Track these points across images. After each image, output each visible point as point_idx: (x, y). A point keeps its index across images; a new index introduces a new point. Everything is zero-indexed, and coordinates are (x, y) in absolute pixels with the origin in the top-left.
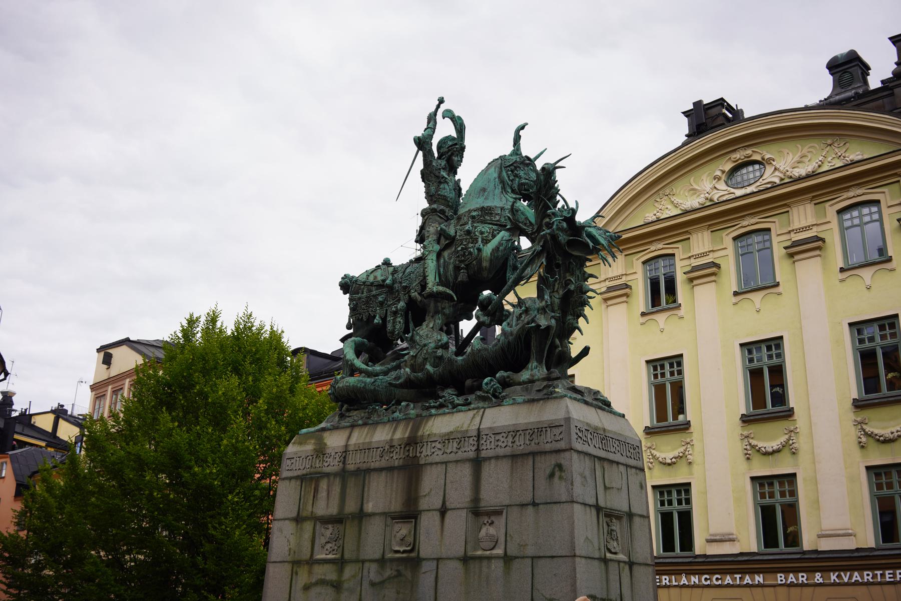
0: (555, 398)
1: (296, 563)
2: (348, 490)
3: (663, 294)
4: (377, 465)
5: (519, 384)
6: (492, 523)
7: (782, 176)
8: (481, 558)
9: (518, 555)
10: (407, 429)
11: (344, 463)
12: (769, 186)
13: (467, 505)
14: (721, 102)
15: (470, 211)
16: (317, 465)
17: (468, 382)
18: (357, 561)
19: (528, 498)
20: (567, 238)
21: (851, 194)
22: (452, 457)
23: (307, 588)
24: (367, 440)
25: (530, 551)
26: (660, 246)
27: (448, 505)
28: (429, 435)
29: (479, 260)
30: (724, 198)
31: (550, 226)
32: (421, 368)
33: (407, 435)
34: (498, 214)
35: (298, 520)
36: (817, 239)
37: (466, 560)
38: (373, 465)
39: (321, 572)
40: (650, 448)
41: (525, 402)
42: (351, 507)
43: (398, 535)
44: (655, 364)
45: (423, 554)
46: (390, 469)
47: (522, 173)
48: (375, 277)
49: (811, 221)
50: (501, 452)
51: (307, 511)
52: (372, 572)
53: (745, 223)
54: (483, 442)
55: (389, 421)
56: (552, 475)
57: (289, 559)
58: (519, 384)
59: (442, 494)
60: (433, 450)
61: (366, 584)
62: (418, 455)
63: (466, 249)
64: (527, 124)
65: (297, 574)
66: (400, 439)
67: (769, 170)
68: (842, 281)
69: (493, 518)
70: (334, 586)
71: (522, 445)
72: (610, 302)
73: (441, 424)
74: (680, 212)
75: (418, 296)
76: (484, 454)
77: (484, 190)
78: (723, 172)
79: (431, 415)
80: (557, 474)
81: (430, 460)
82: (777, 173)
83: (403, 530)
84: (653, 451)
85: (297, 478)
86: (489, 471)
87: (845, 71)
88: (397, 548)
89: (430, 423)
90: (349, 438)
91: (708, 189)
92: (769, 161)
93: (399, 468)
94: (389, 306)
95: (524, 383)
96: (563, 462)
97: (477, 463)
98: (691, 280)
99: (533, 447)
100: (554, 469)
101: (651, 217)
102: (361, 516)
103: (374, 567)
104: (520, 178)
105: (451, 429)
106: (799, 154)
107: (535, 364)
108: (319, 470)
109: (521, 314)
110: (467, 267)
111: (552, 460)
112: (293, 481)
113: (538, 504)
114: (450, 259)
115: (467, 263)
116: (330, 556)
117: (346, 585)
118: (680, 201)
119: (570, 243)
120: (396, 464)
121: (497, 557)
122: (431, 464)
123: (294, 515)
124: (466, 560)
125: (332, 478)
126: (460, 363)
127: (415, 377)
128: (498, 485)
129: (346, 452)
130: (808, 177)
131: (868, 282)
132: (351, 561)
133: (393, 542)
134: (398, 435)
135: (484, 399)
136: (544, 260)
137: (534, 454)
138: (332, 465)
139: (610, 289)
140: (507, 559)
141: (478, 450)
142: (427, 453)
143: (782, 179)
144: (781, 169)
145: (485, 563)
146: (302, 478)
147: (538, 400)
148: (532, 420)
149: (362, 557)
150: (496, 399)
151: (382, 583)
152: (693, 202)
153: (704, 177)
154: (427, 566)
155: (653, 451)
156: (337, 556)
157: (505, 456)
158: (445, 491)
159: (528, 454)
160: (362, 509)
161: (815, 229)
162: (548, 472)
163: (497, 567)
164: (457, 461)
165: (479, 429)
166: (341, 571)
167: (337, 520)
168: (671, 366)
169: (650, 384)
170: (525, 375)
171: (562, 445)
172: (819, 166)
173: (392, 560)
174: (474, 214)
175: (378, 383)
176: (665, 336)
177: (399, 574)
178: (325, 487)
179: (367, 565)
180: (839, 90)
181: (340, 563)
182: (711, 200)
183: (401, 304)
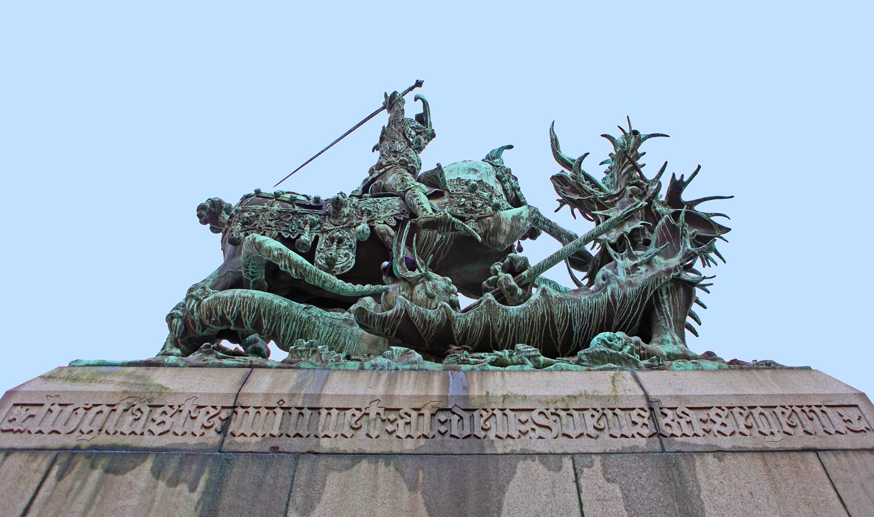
4: (343, 445)
10: (429, 383)
11: (223, 431)
16: (126, 429)
28: (505, 397)
33: (436, 390)
60: (523, 428)
64: (510, 147)
66: (411, 397)
75: (390, 229)
109: (636, 265)
120: (409, 446)
127: (419, 312)
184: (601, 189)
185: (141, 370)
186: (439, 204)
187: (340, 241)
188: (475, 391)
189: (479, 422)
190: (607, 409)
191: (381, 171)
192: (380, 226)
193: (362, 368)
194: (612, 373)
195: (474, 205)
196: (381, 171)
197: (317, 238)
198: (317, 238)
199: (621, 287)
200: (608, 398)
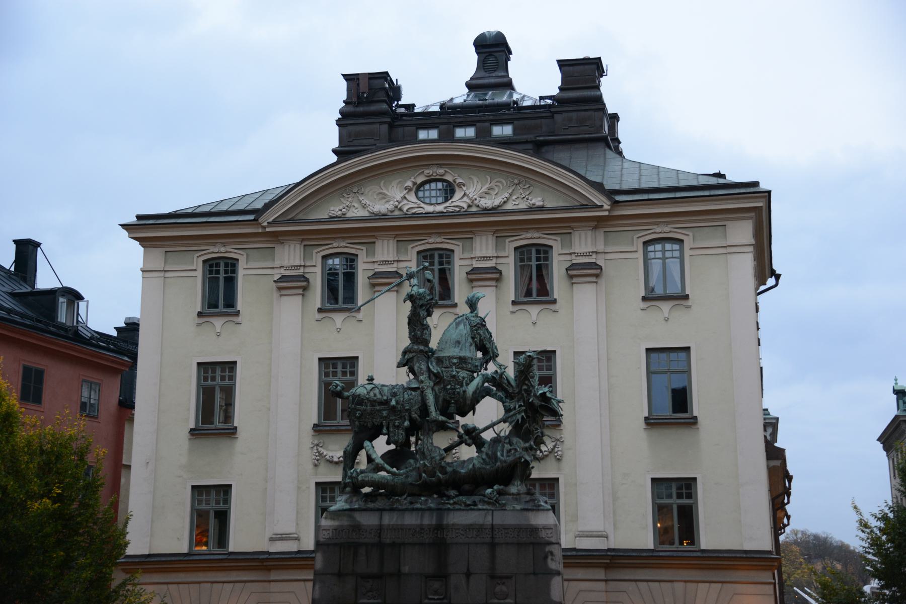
3: (340, 292)
5: (510, 494)
7: (469, 202)
11: (380, 537)
12: (457, 209)
14: (385, 76)
15: (450, 358)
21: (529, 235)
24: (399, 523)
26: (343, 244)
29: (465, 398)
30: (413, 211)
31: (528, 392)
33: (434, 522)
35: (340, 575)
36: (495, 270)
40: (317, 445)
44: (327, 363)
47: (481, 332)
48: (375, 395)
49: (491, 252)
53: (431, 240)
58: (510, 494)
67: (458, 195)
68: (513, 313)
72: (284, 292)
73: (459, 518)
74: (367, 214)
76: (496, 541)
77: (458, 342)
78: (414, 184)
82: (465, 199)
84: (320, 449)
87: (490, 54)
89: (451, 514)
91: (398, 197)
92: (460, 185)
95: (513, 494)
97: (493, 546)
98: (373, 285)
101: (335, 209)
106: (487, 186)
109: (510, 450)
110: (456, 402)
118: (368, 203)
119: (541, 406)
120: (427, 541)
130: (494, 211)
131: (534, 318)
134: (426, 521)
135: (489, 503)
137: (533, 544)
139: (283, 278)
141: (492, 538)
143: (469, 206)
144: (471, 196)
147: (532, 510)
150: (496, 504)
152: (381, 207)
153: (394, 183)
155: (320, 449)
160: (399, 570)
161: (494, 260)
164: (477, 544)
168: (344, 367)
169: (320, 380)
170: (513, 489)
171: (553, 540)
172: (505, 202)
174: (455, 361)
175: (396, 480)
176: (339, 337)
180: (482, 74)
182: (400, 209)
183: (407, 423)
187: (398, 427)
188: (445, 523)
190: (480, 528)
191: (411, 355)
192: (414, 415)
193: (413, 509)
195: (454, 393)
196: (411, 355)
200: (481, 525)
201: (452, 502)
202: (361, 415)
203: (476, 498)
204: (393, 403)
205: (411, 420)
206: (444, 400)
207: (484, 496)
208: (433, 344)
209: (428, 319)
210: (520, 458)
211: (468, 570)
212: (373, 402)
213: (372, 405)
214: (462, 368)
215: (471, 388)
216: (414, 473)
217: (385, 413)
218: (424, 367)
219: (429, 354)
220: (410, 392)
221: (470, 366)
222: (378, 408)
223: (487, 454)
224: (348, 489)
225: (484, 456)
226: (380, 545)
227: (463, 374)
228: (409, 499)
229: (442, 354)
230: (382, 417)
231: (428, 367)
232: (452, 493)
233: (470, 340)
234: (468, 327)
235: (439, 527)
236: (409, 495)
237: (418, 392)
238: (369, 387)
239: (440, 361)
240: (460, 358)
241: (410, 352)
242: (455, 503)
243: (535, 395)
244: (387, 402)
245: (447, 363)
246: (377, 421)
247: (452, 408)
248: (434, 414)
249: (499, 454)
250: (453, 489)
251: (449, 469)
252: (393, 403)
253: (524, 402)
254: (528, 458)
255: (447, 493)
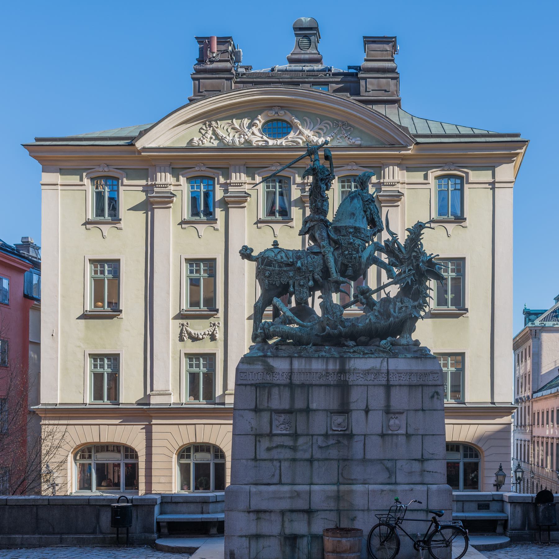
0: (430, 358)
1: (258, 436)
2: (296, 396)
4: (317, 382)
5: (400, 345)
6: (397, 418)
8: (392, 435)
9: (414, 433)
10: (336, 363)
11: (290, 379)
13: (382, 408)
15: (346, 228)
16: (268, 379)
17: (363, 339)
18: (307, 435)
19: (419, 407)
20: (427, 268)
22: (371, 383)
23: (269, 449)
24: (308, 367)
25: (421, 432)
27: (370, 407)
28: (354, 369)
29: (360, 264)
31: (417, 258)
32: (335, 328)
33: (338, 368)
34: (363, 233)
35: (256, 410)
37: (383, 435)
38: (314, 383)
39: (278, 441)
41: (412, 358)
42: (299, 404)
43: (336, 422)
45: (354, 432)
46: (328, 386)
47: (372, 207)
48: (282, 258)
50: (402, 383)
51: (265, 405)
52: (320, 441)
54: (391, 376)
55: (319, 357)
56: (432, 397)
57: (251, 433)
58: (400, 345)
59: (366, 402)
61: (315, 447)
62: (347, 379)
63: (352, 254)
65: (260, 441)
69: (397, 415)
70: (291, 448)
71: (414, 380)
73: (360, 364)
76: (391, 383)
79: (350, 358)
80: (436, 396)
81: (356, 383)
83: (339, 419)
85: (251, 385)
86: (394, 392)
88: (334, 429)
89: (352, 362)
90: (291, 364)
93: (334, 386)
94: (296, 280)
95: (403, 345)
96: (439, 391)
97: (388, 387)
99: (421, 382)
100: (434, 394)
102: (307, 411)
103: (320, 439)
104: (371, 210)
105: (369, 367)
107: (408, 335)
108: (270, 382)
109: (402, 308)
111: (433, 390)
112: (248, 388)
113: (425, 410)
114: (339, 257)
115: (352, 263)
116: (284, 432)
117: (300, 448)
119: (427, 271)
120: (332, 383)
121: (403, 435)
122: (357, 385)
123: (253, 407)
124: (383, 435)
125: (282, 388)
126: (360, 328)
128: (400, 398)
129: (291, 372)
132: (302, 435)
133: (333, 426)
134: (331, 366)
135: (384, 352)
136: (412, 277)
137: (422, 386)
138: (284, 380)
140: (408, 436)
141: (388, 380)
142: (352, 379)
145: (395, 437)
146: (257, 386)
148: (420, 368)
149: (311, 433)
151: (328, 447)
154: (356, 438)
156: (291, 432)
157: (405, 385)
158: (367, 400)
159: (420, 385)
160: (308, 407)
162: (431, 395)
163: (402, 440)
164: (374, 385)
165: (388, 369)
166: (296, 440)
167: (289, 412)
171: (439, 383)
173: (333, 435)
174: (352, 230)
177: (339, 442)
178: (277, 392)
179: (315, 437)
181: (295, 436)
184: (402, 252)
185: (263, 358)
186: (337, 255)
189: (347, 376)
190: (377, 373)
192: (317, 276)
193: (319, 357)
194: (382, 359)
195: (351, 258)
196: (312, 224)
197: (294, 282)
198: (294, 282)
199: (394, 318)
201: (352, 351)
202: (270, 275)
203: (373, 348)
204: (299, 264)
205: (314, 280)
206: (343, 264)
207: (379, 346)
208: (330, 217)
209: (326, 192)
210: (411, 314)
211: (367, 406)
212: (281, 264)
213: (280, 267)
214: (357, 237)
215: (365, 255)
216: (317, 326)
217: (291, 274)
218: (325, 234)
219: (326, 223)
220: (312, 256)
221: (363, 236)
222: (285, 269)
223: (379, 312)
224: (258, 339)
225: (376, 314)
226: (291, 386)
227: (358, 242)
228: (314, 347)
229: (339, 225)
230: (290, 278)
231: (328, 235)
232: (351, 343)
233: (363, 213)
234: (361, 202)
235: (343, 371)
236: (314, 345)
237: (320, 256)
238: (276, 251)
239: (337, 230)
240: (355, 228)
241: (311, 221)
242: (354, 352)
243: (423, 261)
244: (292, 264)
245: (343, 232)
246: (284, 280)
247: (350, 272)
248: (335, 275)
249: (392, 311)
250: (351, 340)
251: (347, 324)
252: (299, 264)
253: (413, 266)
254: (417, 315)
255: (346, 343)
